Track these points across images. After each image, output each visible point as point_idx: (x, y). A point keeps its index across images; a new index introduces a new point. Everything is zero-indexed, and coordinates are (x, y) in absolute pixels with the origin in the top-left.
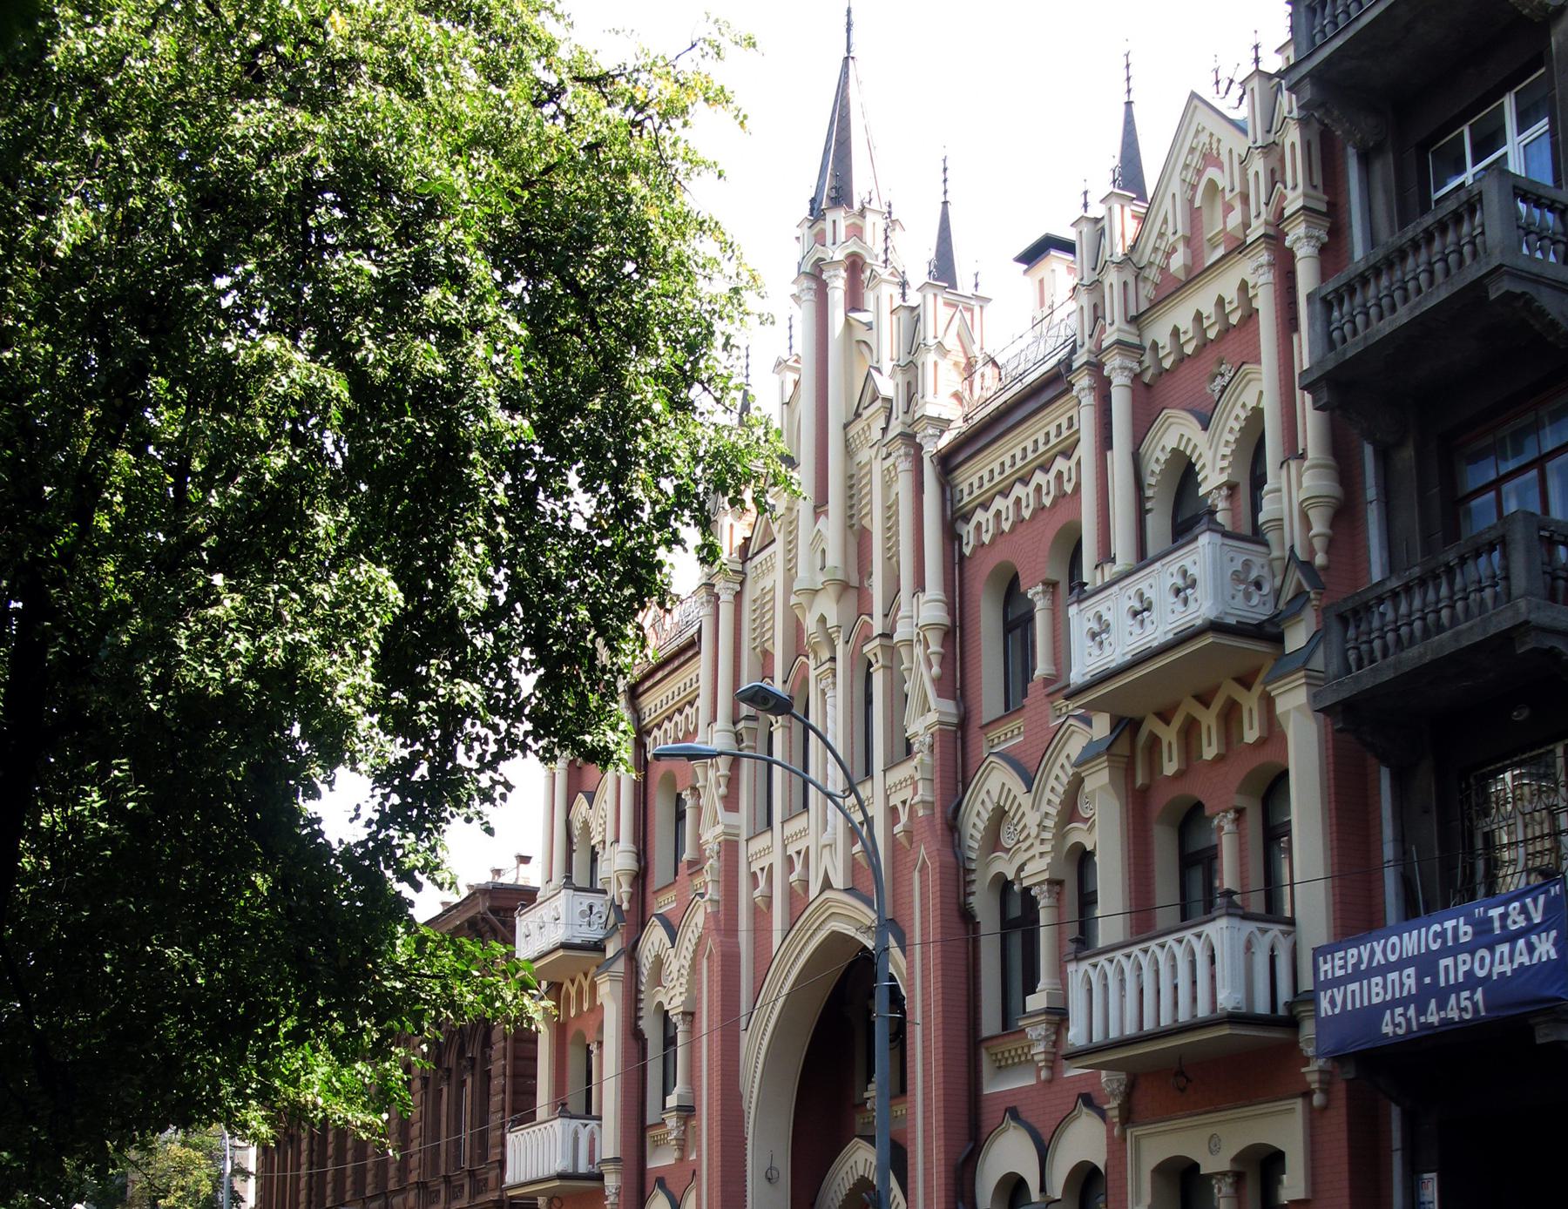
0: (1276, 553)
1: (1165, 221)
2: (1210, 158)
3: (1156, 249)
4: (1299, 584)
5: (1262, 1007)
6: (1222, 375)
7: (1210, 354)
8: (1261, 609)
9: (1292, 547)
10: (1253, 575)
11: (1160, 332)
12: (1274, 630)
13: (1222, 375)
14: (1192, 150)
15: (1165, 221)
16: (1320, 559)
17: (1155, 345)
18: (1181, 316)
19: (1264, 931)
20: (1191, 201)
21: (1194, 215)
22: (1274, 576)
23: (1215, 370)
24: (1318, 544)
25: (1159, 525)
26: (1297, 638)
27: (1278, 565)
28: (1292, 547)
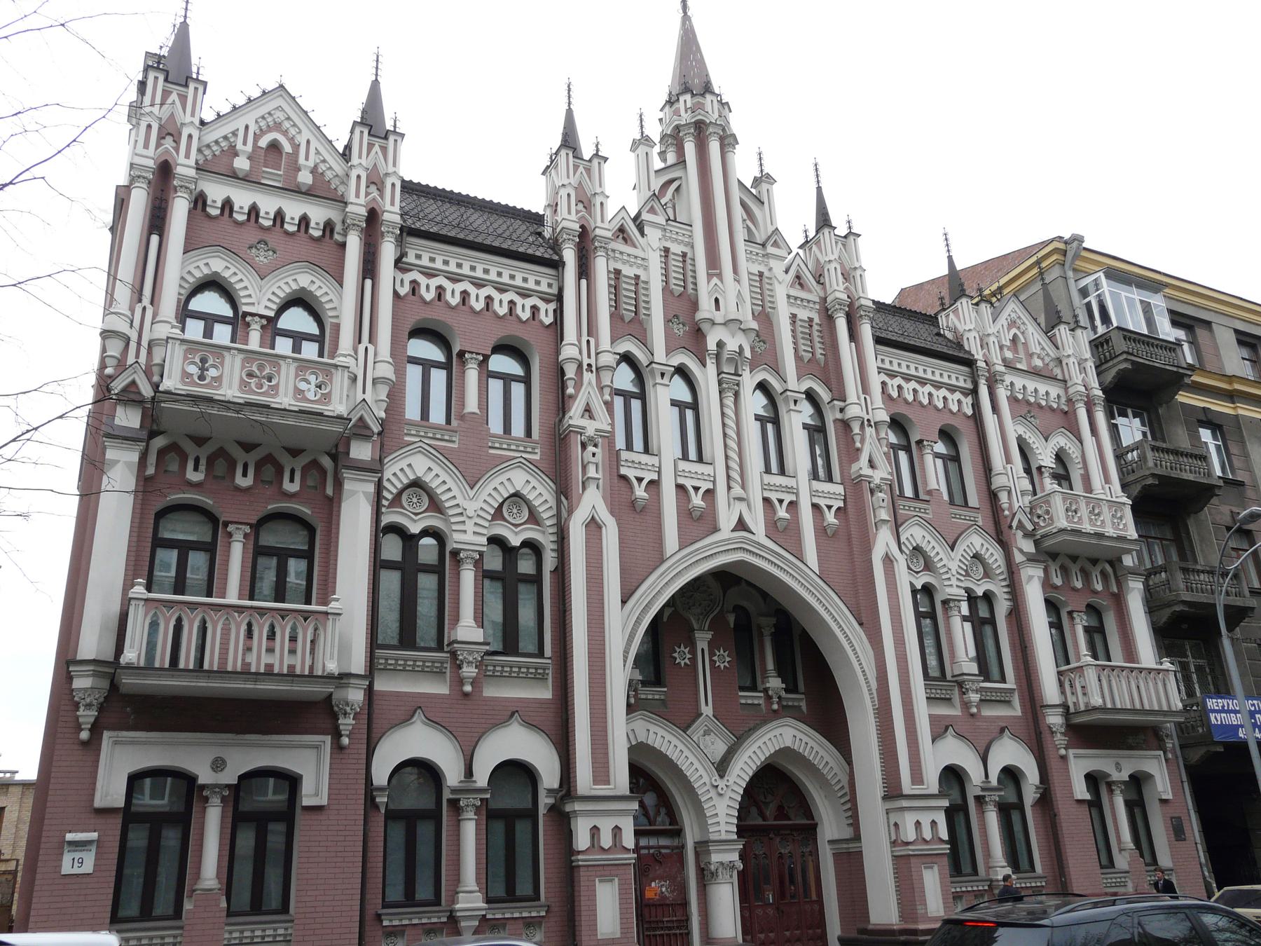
3: (217, 142)
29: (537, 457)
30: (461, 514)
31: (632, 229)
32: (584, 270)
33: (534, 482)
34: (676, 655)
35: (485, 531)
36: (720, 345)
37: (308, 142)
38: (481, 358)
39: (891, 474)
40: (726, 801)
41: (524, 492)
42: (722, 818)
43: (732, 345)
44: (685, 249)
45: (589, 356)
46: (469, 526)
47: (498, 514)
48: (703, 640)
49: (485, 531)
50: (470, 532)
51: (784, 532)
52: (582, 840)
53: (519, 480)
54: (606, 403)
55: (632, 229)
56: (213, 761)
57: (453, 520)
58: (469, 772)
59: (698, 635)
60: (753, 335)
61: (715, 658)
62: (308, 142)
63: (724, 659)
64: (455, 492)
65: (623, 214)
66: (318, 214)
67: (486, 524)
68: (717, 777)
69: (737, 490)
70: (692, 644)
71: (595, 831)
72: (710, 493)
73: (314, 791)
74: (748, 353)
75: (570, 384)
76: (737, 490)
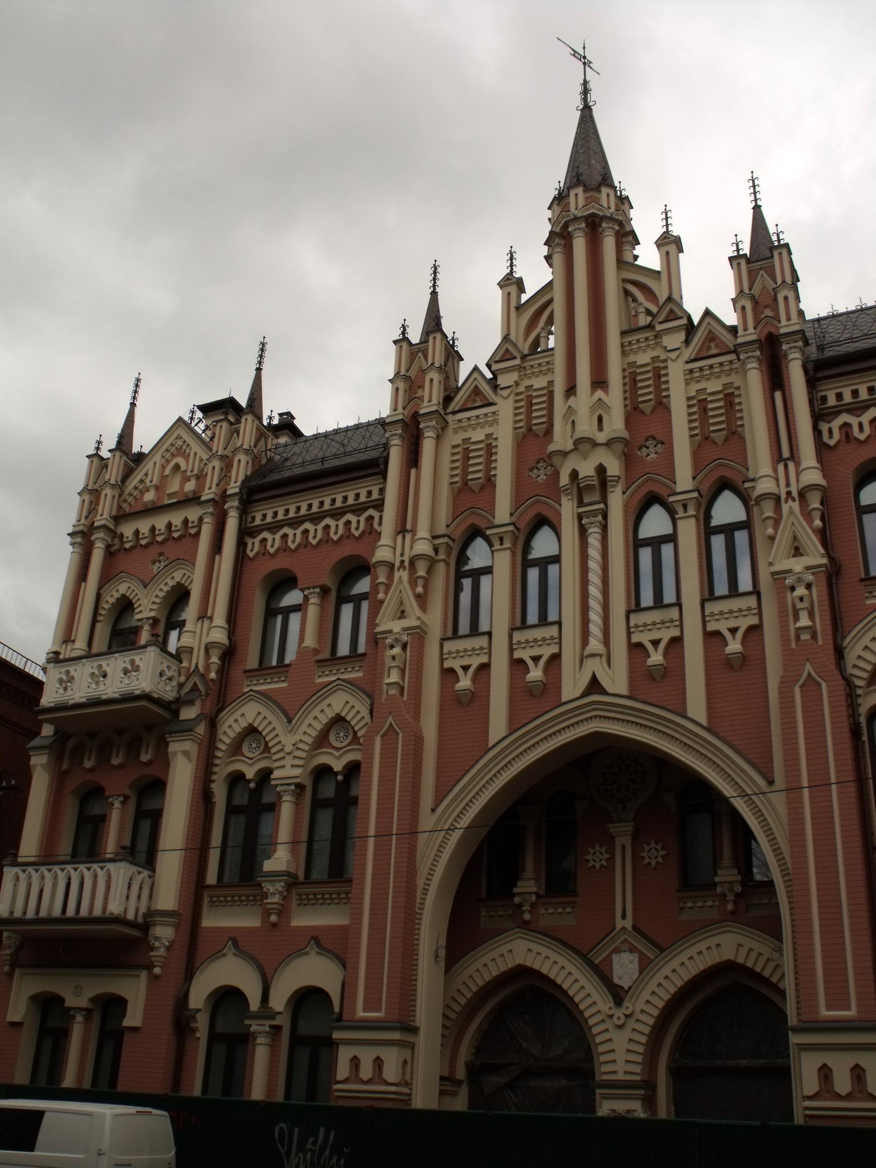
0: (185, 664)
1: (146, 475)
2: (181, 452)
3: (136, 488)
4: (195, 684)
5: (130, 916)
6: (160, 562)
7: (154, 551)
8: (170, 693)
9: (197, 666)
10: (169, 674)
11: (128, 530)
12: (174, 707)
13: (160, 562)
14: (172, 445)
15: (146, 475)
16: (213, 675)
17: (122, 535)
18: (144, 526)
19: (139, 873)
20: (163, 467)
21: (164, 478)
22: (180, 676)
23: (157, 558)
24: (214, 668)
25: (103, 631)
26: (188, 713)
27: (183, 671)
28: (197, 666)
29: (360, 674)
30: (282, 750)
31: (486, 389)
32: (413, 459)
33: (353, 701)
34: (589, 857)
35: (301, 762)
36: (574, 475)
37: (196, 453)
38: (318, 590)
39: (823, 556)
40: (627, 1033)
41: (343, 714)
42: (620, 1055)
43: (587, 469)
44: (549, 378)
45: (402, 555)
46: (289, 761)
47: (322, 740)
48: (622, 834)
49: (301, 762)
50: (288, 766)
51: (658, 681)
52: (343, 1070)
53: (338, 703)
54: (418, 597)
55: (486, 389)
56: (78, 992)
57: (275, 757)
58: (265, 998)
59: (614, 828)
60: (619, 447)
61: (644, 854)
62: (196, 453)
63: (654, 854)
64: (279, 730)
65: (476, 375)
66: (193, 514)
67: (303, 755)
68: (612, 1004)
69: (595, 645)
70: (609, 841)
71: (355, 1062)
72: (556, 658)
73: (133, 1018)
74: (614, 468)
75: (382, 588)
76: (595, 645)
